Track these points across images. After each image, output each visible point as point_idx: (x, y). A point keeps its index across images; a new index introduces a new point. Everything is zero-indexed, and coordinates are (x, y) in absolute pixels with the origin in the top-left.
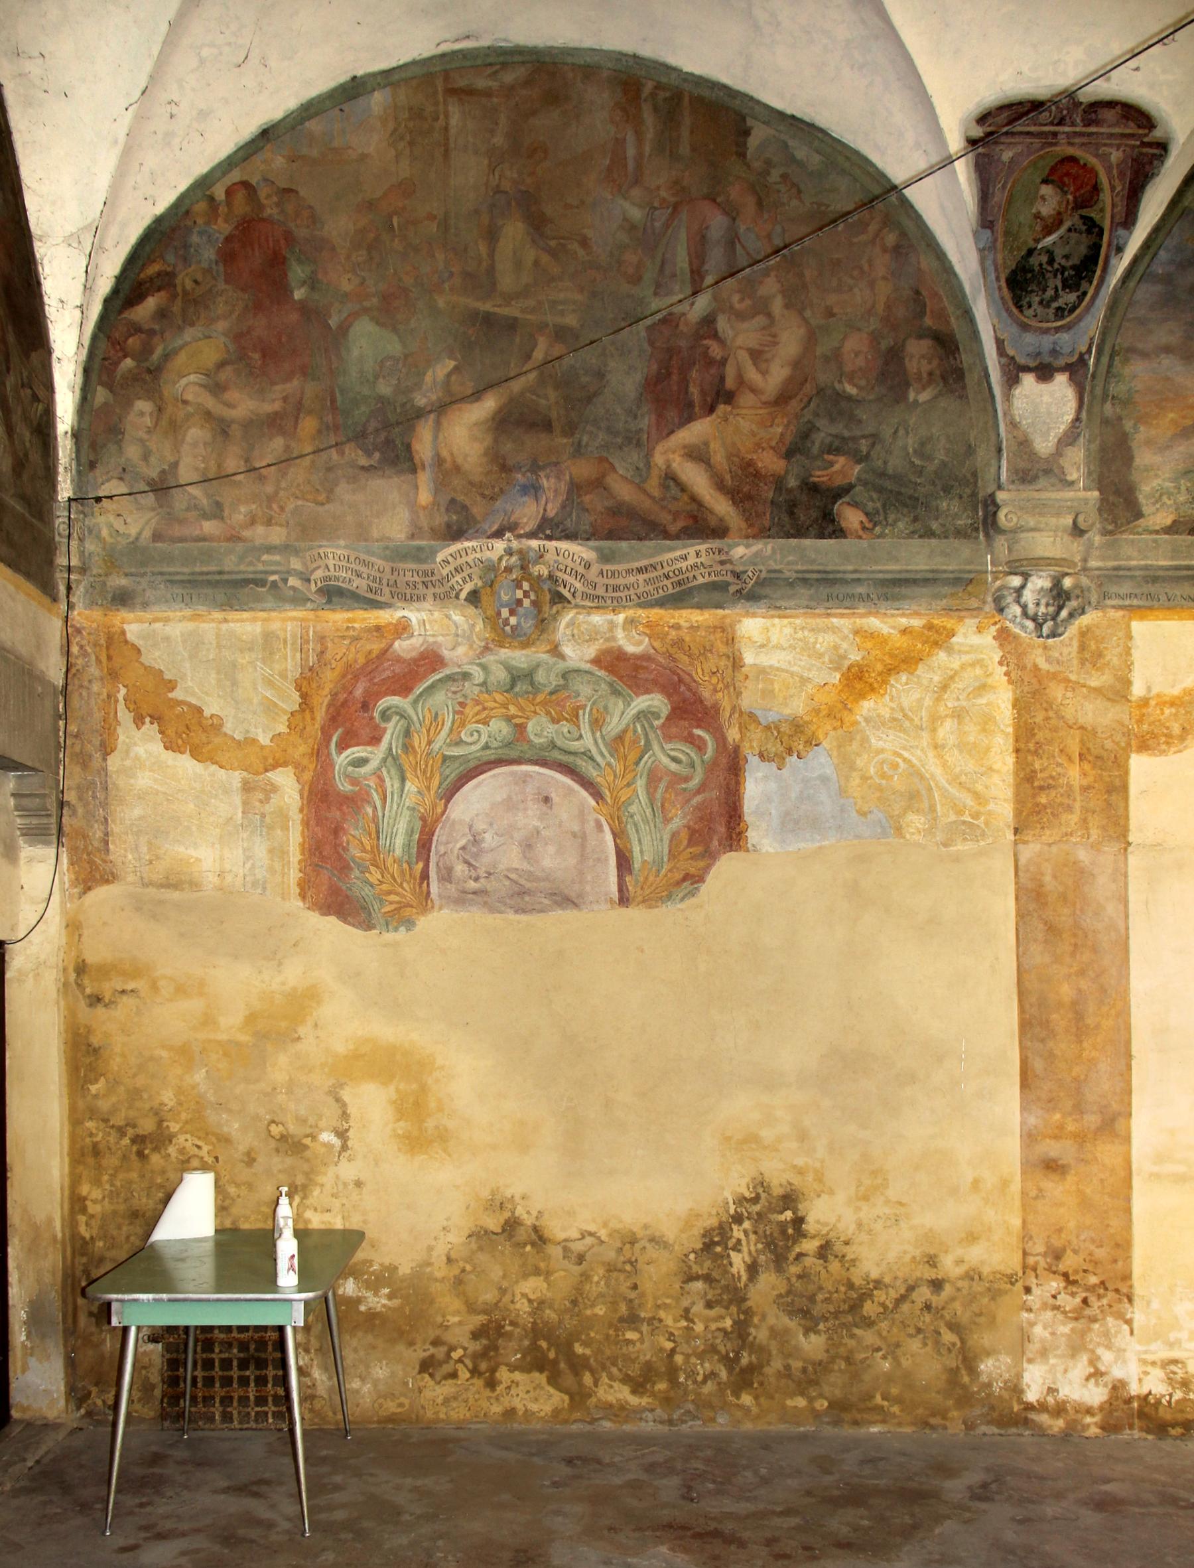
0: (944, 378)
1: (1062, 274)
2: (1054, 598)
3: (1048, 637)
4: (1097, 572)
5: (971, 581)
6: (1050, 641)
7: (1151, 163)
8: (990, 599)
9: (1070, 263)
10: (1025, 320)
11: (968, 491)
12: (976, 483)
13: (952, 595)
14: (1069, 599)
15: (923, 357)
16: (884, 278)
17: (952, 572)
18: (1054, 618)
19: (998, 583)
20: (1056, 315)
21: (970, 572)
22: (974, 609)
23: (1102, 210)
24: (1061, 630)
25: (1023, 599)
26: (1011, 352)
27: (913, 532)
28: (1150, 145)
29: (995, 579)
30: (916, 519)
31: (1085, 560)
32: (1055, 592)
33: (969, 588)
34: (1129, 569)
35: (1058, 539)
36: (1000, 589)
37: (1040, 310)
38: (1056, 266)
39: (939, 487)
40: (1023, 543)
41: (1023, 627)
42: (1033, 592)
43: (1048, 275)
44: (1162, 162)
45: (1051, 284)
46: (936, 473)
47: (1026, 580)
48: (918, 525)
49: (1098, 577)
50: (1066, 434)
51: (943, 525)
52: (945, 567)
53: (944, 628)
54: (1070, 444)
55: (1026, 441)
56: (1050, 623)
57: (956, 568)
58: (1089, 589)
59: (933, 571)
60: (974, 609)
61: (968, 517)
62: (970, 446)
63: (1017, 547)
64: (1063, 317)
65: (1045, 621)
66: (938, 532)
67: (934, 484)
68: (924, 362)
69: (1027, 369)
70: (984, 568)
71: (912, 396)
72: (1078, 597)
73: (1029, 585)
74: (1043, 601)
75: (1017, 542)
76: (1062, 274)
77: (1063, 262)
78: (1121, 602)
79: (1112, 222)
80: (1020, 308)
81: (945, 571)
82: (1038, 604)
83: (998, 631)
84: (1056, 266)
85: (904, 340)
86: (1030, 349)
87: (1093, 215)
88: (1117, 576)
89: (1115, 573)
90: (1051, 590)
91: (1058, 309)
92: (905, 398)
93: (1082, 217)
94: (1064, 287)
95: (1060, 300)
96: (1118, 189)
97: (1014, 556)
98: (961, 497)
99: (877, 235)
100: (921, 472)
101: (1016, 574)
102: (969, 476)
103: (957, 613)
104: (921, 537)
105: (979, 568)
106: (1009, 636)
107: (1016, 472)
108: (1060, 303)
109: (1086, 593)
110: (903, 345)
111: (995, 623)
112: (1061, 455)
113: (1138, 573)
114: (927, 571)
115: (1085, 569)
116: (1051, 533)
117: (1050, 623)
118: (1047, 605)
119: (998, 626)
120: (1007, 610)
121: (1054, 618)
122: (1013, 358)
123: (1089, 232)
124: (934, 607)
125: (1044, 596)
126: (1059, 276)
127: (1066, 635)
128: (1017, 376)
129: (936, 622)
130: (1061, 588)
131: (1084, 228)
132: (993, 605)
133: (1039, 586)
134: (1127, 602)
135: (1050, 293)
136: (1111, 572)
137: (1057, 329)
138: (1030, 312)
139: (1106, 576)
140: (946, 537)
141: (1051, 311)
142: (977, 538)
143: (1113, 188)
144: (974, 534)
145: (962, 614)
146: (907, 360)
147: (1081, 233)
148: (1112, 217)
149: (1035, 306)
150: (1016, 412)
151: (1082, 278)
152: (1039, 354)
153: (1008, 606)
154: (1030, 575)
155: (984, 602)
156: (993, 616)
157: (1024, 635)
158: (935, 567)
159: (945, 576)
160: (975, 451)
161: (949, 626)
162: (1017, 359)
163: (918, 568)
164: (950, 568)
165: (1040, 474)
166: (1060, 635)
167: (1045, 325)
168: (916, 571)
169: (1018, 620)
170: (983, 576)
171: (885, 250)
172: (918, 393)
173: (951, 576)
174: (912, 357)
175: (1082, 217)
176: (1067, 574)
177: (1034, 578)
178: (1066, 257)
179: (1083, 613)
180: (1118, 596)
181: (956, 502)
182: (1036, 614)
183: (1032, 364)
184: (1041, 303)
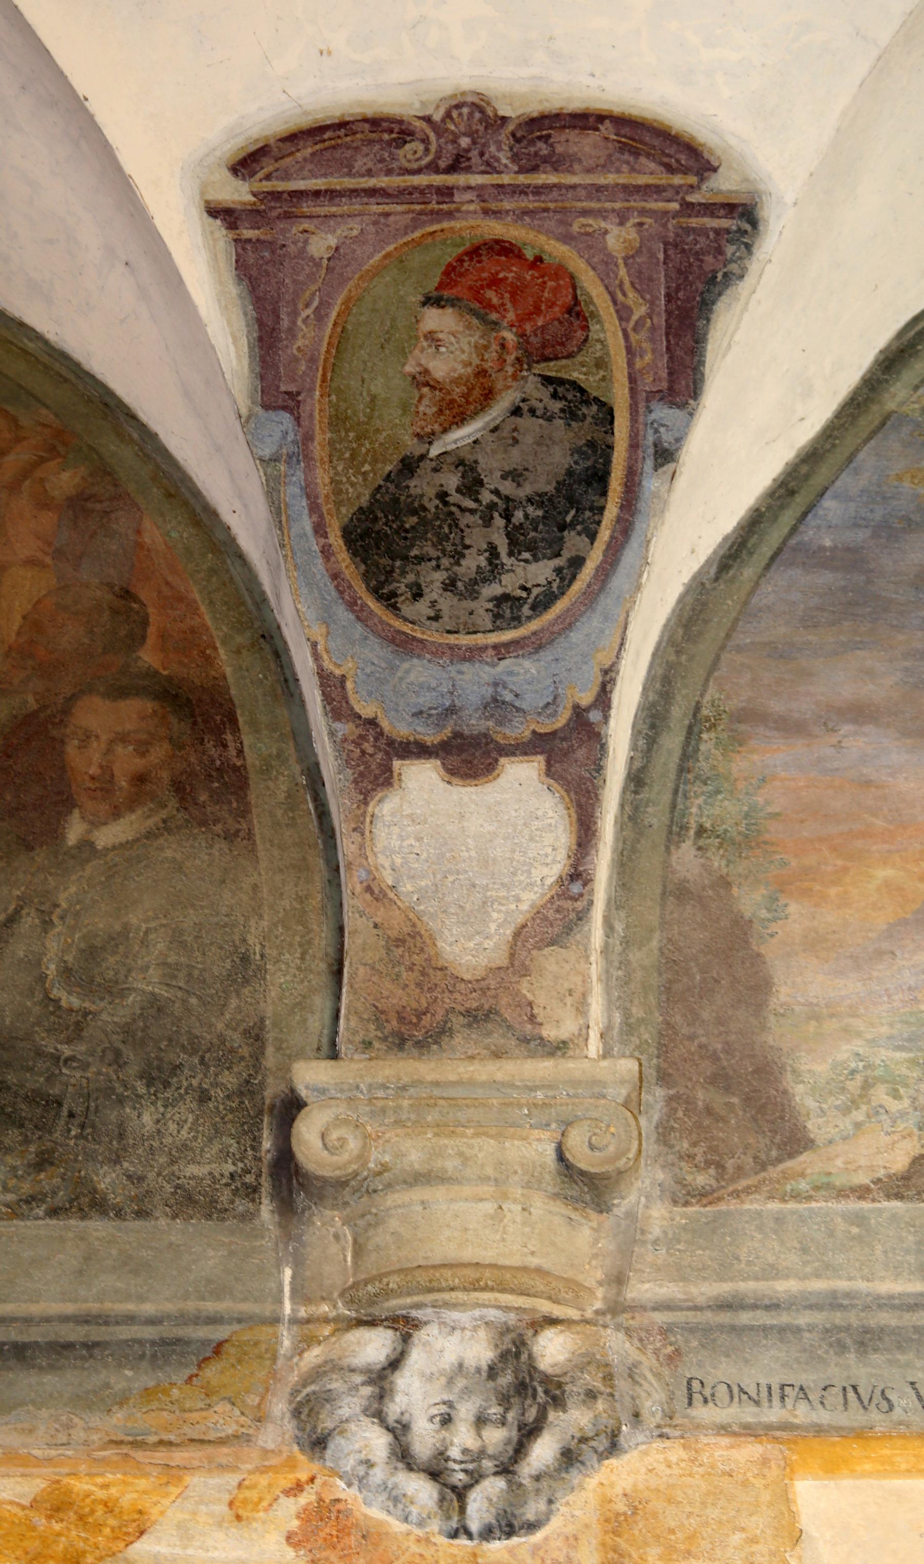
0: (178, 787)
1: (507, 516)
2: (505, 1400)
3: (487, 1533)
4: (660, 1318)
5: (218, 1349)
6: (497, 1546)
7: (719, 251)
8: (280, 1407)
9: (527, 490)
10: (407, 628)
11: (229, 1079)
12: (257, 1057)
13: (148, 1394)
14: (558, 1402)
15: (123, 738)
16: (32, 562)
17: (152, 1321)
18: (506, 1470)
19: (314, 1356)
20: (497, 616)
21: (214, 1320)
22: (222, 1442)
23: (601, 363)
24: (532, 1510)
25: (393, 1410)
26: (366, 710)
27: (30, 1200)
28: (709, 209)
29: (309, 1341)
30: (43, 1162)
31: (618, 1280)
32: (506, 1379)
33: (211, 1373)
34: (773, 1307)
35: (513, 1209)
36: (318, 1373)
37: (447, 603)
38: (486, 497)
39: (132, 1070)
40: (393, 1224)
41: (396, 1499)
42: (429, 1378)
43: (465, 519)
44: (748, 247)
45: (477, 538)
46: (127, 1030)
47: (406, 1338)
48: (47, 1180)
49: (666, 1331)
50: (538, 914)
51: (136, 1179)
52: (130, 1307)
53: (109, 1507)
54: (552, 943)
55: (415, 935)
56: (494, 1486)
57: (170, 1307)
58: (632, 1373)
59: (85, 1320)
60: (222, 1442)
61: (225, 1154)
62: (245, 959)
63: (379, 1237)
64: (517, 621)
65: (476, 1477)
66: (113, 1199)
67: (118, 1060)
68: (124, 752)
69: (420, 751)
70: (267, 1309)
71: (75, 830)
72: (592, 1395)
73: (416, 1358)
74: (466, 1411)
75: (378, 1222)
76: (507, 516)
77: (507, 488)
78: (748, 1414)
79: (633, 391)
80: (389, 600)
81: (130, 1319)
82: (447, 1421)
83: (305, 1515)
84: (486, 497)
85: (72, 699)
86: (426, 700)
87: (575, 375)
88: (733, 1329)
89: (725, 1318)
90: (492, 1372)
91: (505, 598)
92: (55, 834)
93: (547, 380)
94: (515, 546)
95: (506, 579)
96: (640, 311)
97: (371, 1265)
98: (204, 1097)
99: (25, 473)
100: (79, 1027)
101: (372, 1323)
102: (236, 1038)
103: (160, 1456)
104: (54, 1212)
105: (247, 1307)
106: (344, 1531)
107: (379, 1016)
108: (508, 584)
109: (622, 1384)
110: (66, 711)
111: (298, 1488)
112: (525, 972)
113: (803, 1319)
114: (65, 1319)
115: (615, 1308)
116: (487, 1189)
117: (494, 1486)
118: (481, 1421)
119: (307, 1498)
120: (336, 1444)
121: (506, 1470)
122: (372, 722)
123: (571, 414)
124: (79, 1434)
125: (467, 1392)
126: (499, 522)
127: (555, 1523)
128: (388, 769)
129: (80, 1486)
130: (532, 1368)
131: (556, 406)
132: (290, 1426)
133: (449, 1359)
134: (774, 1414)
135: (473, 562)
136: (709, 1317)
137: (502, 651)
138: (422, 608)
139: (691, 1329)
140: (142, 1214)
141: (482, 607)
142: (248, 1217)
143: (623, 313)
144: (241, 1205)
145: (179, 1457)
146: (71, 749)
147: (550, 419)
148: (632, 379)
149: (434, 592)
150: (382, 859)
151: (563, 527)
152: (451, 710)
153: (341, 1428)
154: (416, 1325)
155: (260, 1419)
156: (291, 1464)
157: (397, 1526)
158: (94, 1307)
159: (125, 1333)
160: (261, 970)
161: (127, 1499)
162: (385, 724)
163: (35, 1309)
164: (149, 1309)
165: (457, 1021)
166: (532, 1527)
167: (465, 640)
168: (28, 1321)
169: (378, 1475)
170: (264, 1332)
171: (43, 503)
172: (95, 824)
173: (149, 1333)
174: (87, 737)
175: (547, 380)
176: (552, 1322)
177: (428, 1335)
178: (515, 475)
179: (614, 1447)
180: (736, 1393)
181: (186, 1110)
182: (441, 1455)
183: (431, 737)
184: (450, 585)
